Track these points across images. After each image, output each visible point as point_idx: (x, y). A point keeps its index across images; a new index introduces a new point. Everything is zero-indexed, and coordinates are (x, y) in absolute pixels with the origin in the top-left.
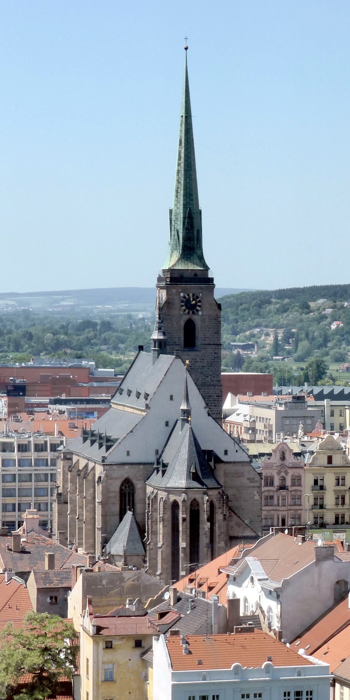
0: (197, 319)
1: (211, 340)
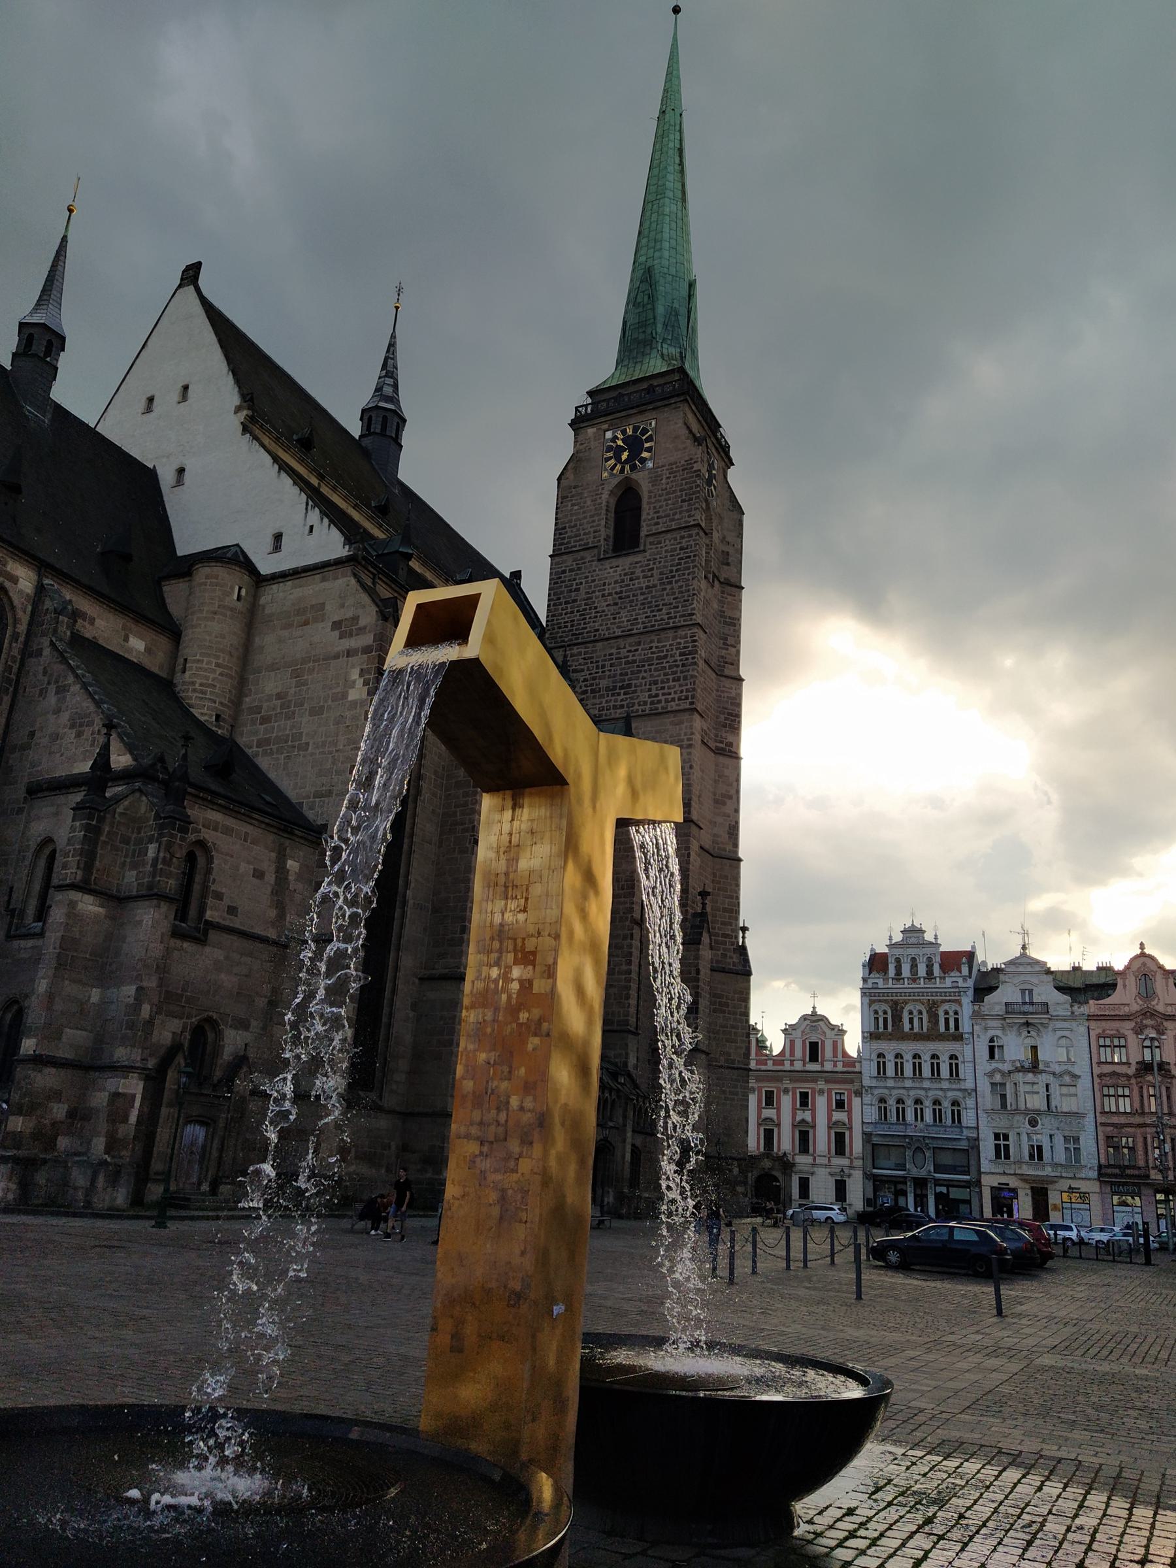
0: (642, 479)
1: (673, 520)
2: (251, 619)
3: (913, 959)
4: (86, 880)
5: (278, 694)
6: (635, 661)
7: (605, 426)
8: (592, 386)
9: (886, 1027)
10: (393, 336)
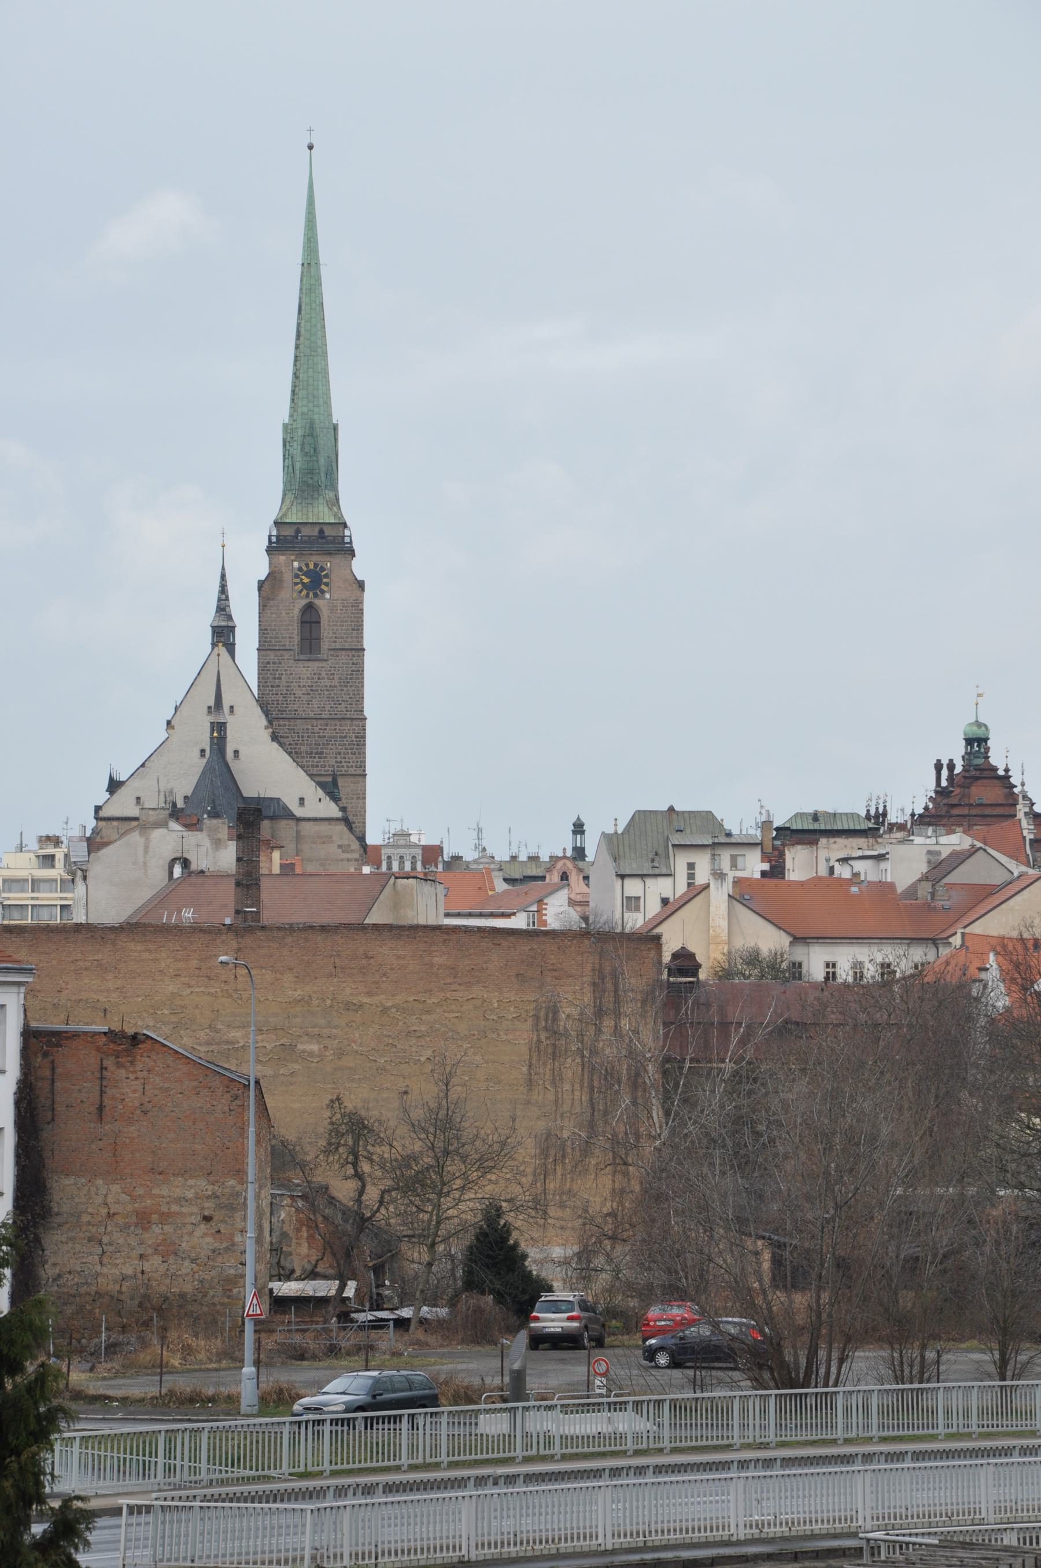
3: (401, 857)
7: (293, 557)
10: (223, 568)
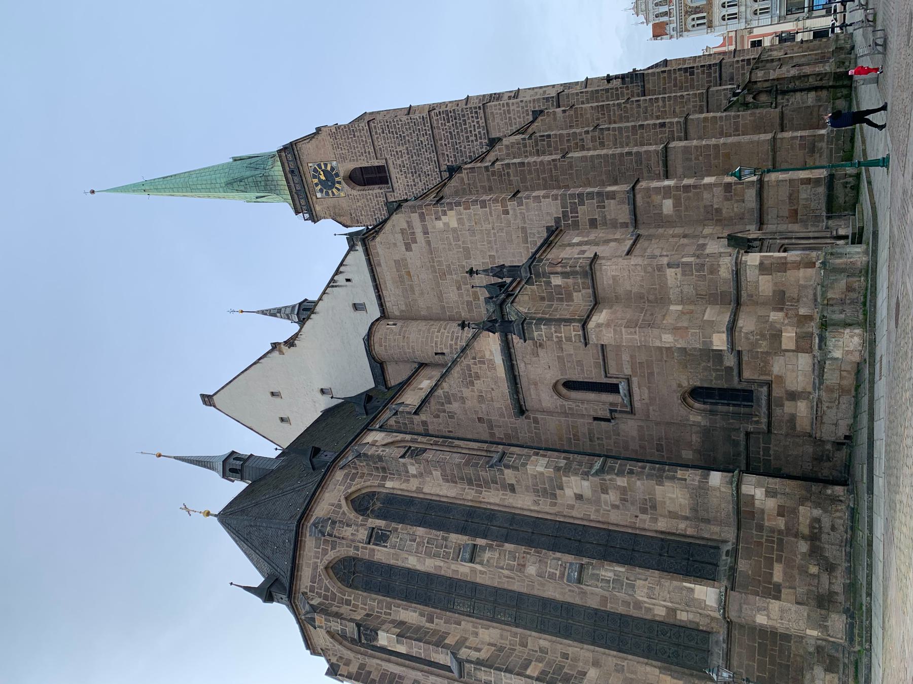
0: (345, 168)
2: (409, 316)
4: (579, 321)
5: (458, 289)
6: (455, 155)
7: (314, 198)
8: (292, 212)
9: (704, 18)
10: (258, 312)
